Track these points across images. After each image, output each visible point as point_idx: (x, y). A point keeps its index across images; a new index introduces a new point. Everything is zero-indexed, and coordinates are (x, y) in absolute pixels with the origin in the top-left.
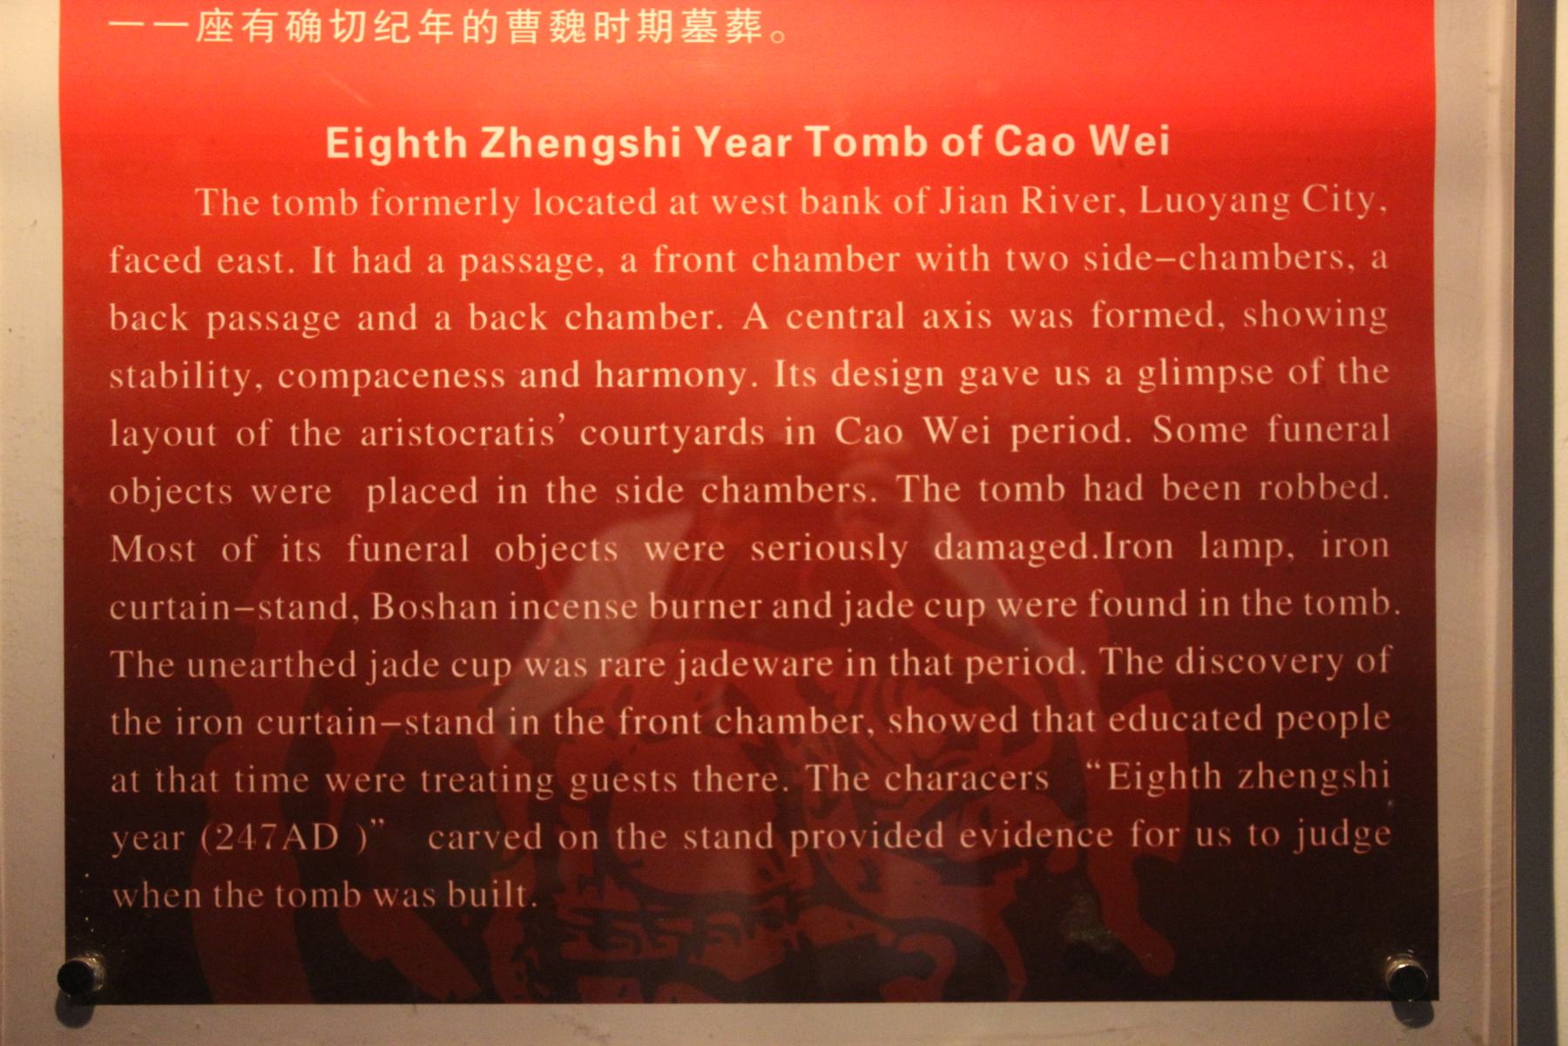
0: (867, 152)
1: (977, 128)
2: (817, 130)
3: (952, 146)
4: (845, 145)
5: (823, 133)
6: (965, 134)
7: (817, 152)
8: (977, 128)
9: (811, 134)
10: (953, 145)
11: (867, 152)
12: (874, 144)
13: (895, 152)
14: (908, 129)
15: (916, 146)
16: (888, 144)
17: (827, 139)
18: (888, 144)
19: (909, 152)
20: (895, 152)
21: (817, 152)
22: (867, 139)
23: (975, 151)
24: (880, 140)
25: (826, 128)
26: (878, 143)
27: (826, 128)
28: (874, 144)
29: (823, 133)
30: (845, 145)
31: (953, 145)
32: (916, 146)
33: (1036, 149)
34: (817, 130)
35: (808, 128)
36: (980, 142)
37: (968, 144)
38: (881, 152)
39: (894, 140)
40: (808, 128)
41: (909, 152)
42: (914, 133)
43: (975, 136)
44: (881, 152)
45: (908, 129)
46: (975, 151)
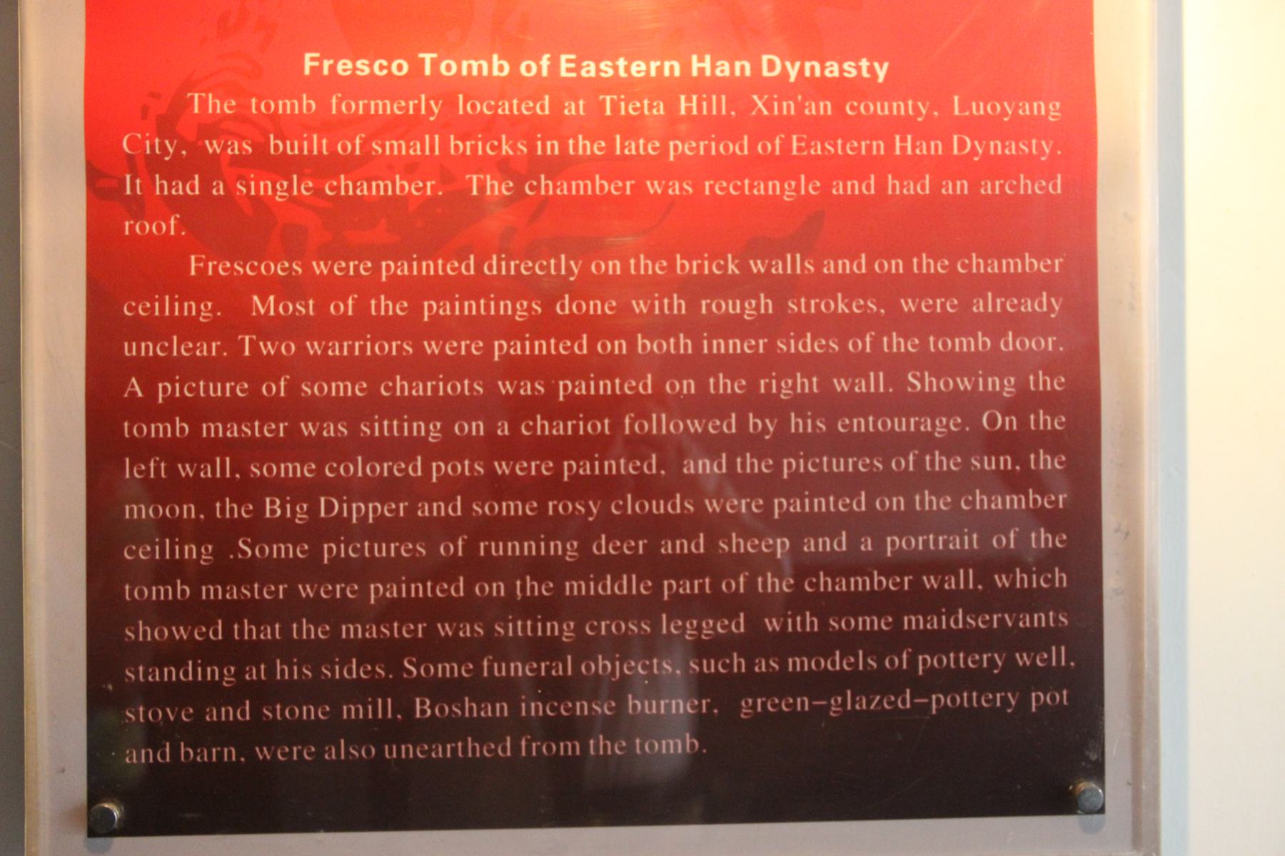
0: (464, 72)
1: (546, 56)
2: (428, 57)
3: (528, 69)
4: (448, 68)
5: (432, 59)
6: (537, 60)
7: (428, 72)
8: (546, 56)
9: (423, 60)
10: (529, 69)
11: (464, 72)
12: (470, 67)
13: (485, 73)
14: (495, 57)
15: (501, 68)
16: (480, 67)
17: (436, 64)
18: (480, 67)
19: (496, 73)
20: (485, 73)
21: (428, 72)
22: (465, 64)
23: (545, 73)
24: (475, 64)
25: (435, 55)
26: (472, 67)
27: (435, 55)
28: (470, 67)
29: (432, 59)
30: (448, 68)
31: (529, 69)
32: (501, 68)
33: (588, 72)
34: (428, 57)
35: (421, 55)
36: (549, 67)
37: (540, 68)
38: (475, 73)
39: (485, 64)
40: (421, 55)
41: (496, 73)
42: (500, 59)
43: (545, 62)
44: (475, 73)
45: (495, 57)
46: (545, 73)
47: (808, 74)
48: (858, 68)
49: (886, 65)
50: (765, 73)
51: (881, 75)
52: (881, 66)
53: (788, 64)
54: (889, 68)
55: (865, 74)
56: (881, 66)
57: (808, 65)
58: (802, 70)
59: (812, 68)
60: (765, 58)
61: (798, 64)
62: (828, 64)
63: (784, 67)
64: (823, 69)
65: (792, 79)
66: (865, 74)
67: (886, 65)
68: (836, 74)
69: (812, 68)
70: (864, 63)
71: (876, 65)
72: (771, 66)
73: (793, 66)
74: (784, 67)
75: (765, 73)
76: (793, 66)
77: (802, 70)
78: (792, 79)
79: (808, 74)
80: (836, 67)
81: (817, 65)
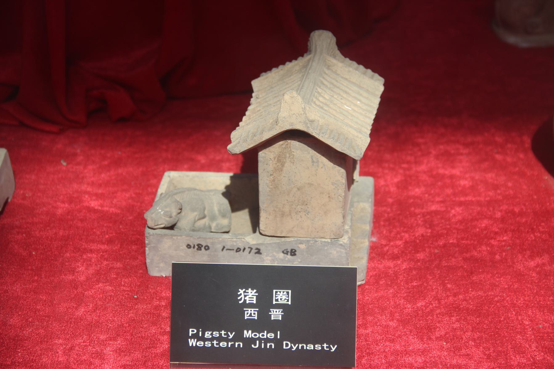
47: (300, 348)
49: (336, 346)
57: (300, 346)
58: (298, 346)
61: (297, 345)
63: (291, 346)
64: (307, 346)
68: (312, 348)
69: (303, 347)
72: (287, 345)
73: (295, 346)
74: (291, 346)
76: (295, 346)
77: (298, 346)
79: (300, 348)
80: (312, 346)
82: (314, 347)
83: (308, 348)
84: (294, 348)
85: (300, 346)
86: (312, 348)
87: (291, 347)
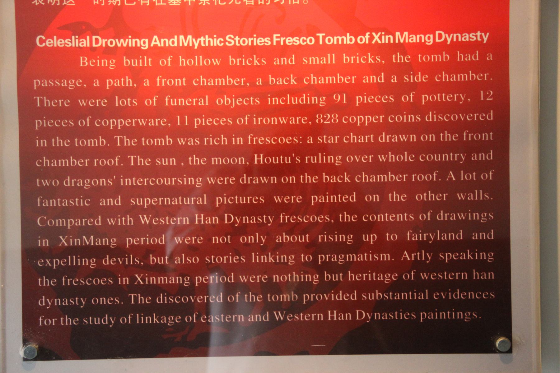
47: (455, 40)
48: (476, 36)
49: (488, 34)
50: (437, 40)
51: (485, 39)
52: (485, 36)
53: (447, 35)
54: (489, 35)
55: (479, 39)
56: (485, 36)
57: (455, 35)
59: (457, 37)
60: (437, 32)
61: (451, 35)
62: (464, 35)
63: (445, 37)
64: (462, 37)
65: (449, 43)
66: (479, 39)
67: (488, 34)
68: (467, 39)
69: (457, 37)
70: (479, 34)
71: (483, 34)
72: (440, 36)
74: (445, 37)
75: (437, 40)
78: (449, 43)
79: (455, 40)
81: (459, 35)
82: (470, 38)
83: (463, 40)
84: (449, 40)
85: (455, 35)
86: (467, 39)
87: (446, 40)
